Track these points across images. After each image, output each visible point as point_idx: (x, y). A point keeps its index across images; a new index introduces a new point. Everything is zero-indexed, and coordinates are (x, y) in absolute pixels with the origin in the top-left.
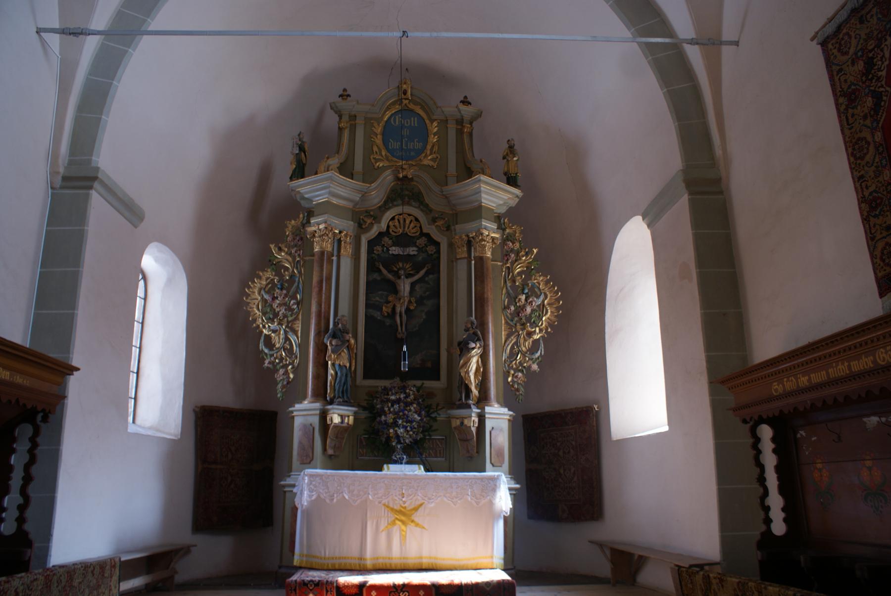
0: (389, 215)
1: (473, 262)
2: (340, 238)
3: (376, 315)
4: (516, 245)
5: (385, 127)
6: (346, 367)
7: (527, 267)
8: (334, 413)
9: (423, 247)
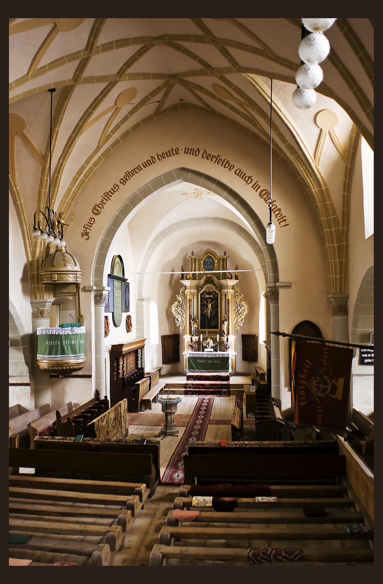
0: (205, 287)
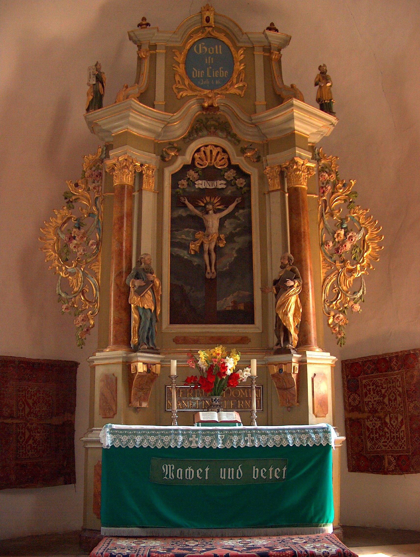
0: (194, 146)
1: (287, 195)
2: (142, 171)
3: (182, 254)
4: (332, 177)
5: (187, 56)
6: (151, 310)
7: (345, 201)
8: (138, 361)
9: (232, 180)
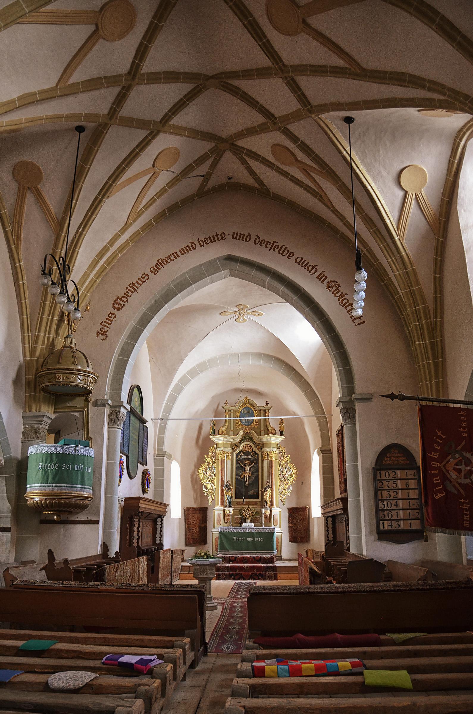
0: (242, 445)
